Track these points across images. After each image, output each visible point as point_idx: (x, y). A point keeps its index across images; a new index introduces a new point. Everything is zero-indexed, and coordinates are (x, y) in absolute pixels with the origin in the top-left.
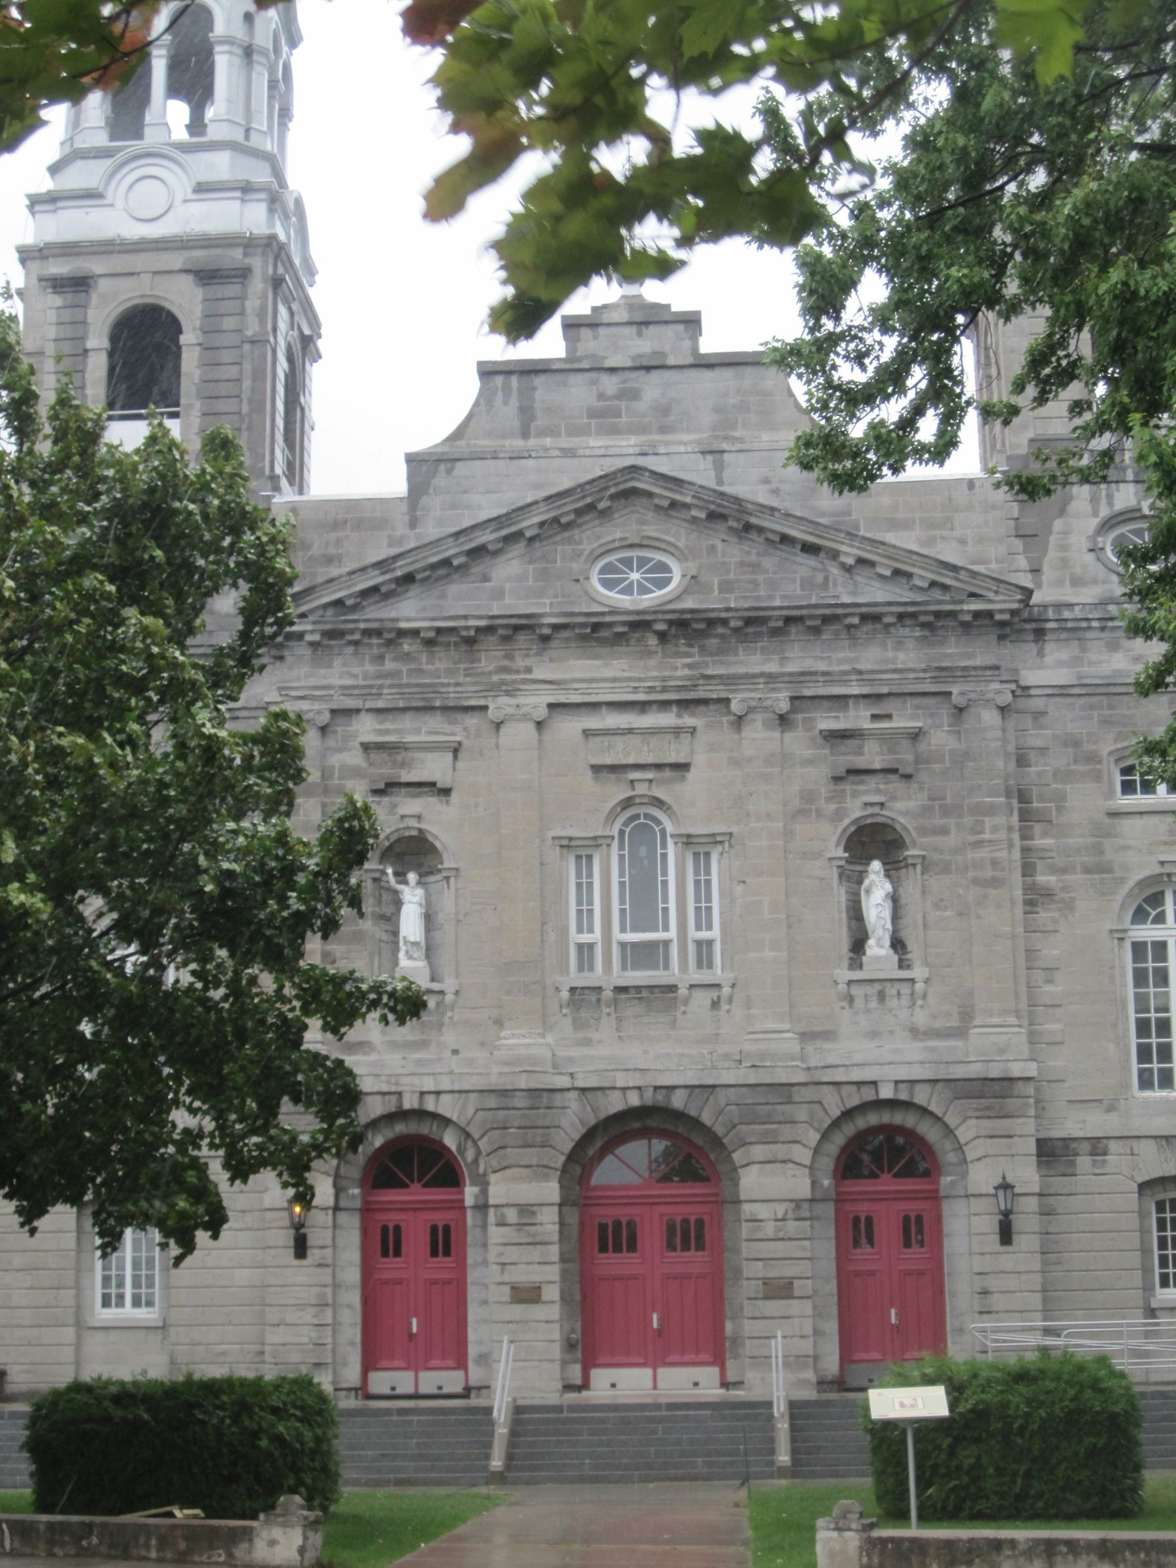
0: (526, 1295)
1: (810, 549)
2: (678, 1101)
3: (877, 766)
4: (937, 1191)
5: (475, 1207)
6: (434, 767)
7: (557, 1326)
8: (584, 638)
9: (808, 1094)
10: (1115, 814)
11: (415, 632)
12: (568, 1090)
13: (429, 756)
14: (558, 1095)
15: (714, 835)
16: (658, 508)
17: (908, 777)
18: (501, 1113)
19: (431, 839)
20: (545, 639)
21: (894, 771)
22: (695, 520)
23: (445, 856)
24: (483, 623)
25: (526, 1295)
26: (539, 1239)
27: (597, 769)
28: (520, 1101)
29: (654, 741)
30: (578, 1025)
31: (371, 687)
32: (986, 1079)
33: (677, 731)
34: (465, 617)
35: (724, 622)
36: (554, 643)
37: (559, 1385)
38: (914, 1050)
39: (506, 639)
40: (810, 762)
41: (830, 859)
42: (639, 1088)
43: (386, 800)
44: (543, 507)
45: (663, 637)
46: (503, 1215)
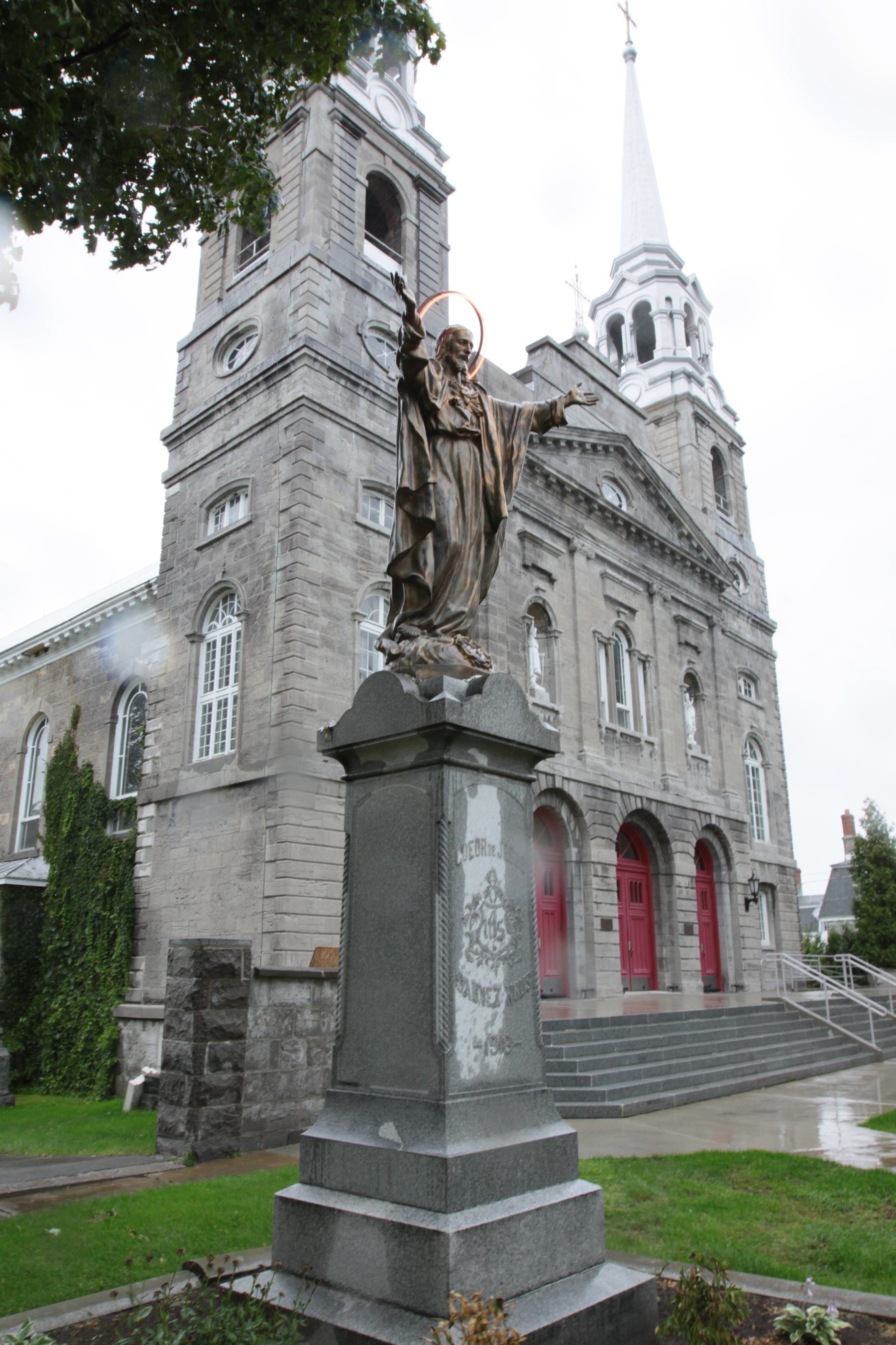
0: (606, 925)
1: (672, 519)
2: (653, 808)
3: (693, 643)
4: (712, 879)
5: (576, 862)
6: (548, 563)
7: (618, 947)
8: (605, 519)
9: (693, 815)
10: (740, 698)
11: (546, 476)
12: (615, 791)
13: (550, 557)
14: (613, 794)
15: (647, 656)
16: (626, 466)
17: (699, 653)
18: (594, 800)
19: (548, 609)
20: (591, 511)
21: (695, 648)
22: (638, 479)
23: (553, 623)
24: (577, 487)
25: (606, 925)
26: (610, 888)
27: (608, 598)
28: (600, 795)
29: (627, 591)
30: (607, 752)
31: (526, 498)
32: (737, 821)
33: (636, 591)
34: (571, 479)
35: (651, 539)
36: (592, 516)
37: (621, 988)
38: (711, 799)
39: (578, 502)
40: (670, 630)
41: (681, 687)
42: (641, 797)
43: (529, 574)
44: (596, 435)
45: (629, 533)
46: (596, 870)
